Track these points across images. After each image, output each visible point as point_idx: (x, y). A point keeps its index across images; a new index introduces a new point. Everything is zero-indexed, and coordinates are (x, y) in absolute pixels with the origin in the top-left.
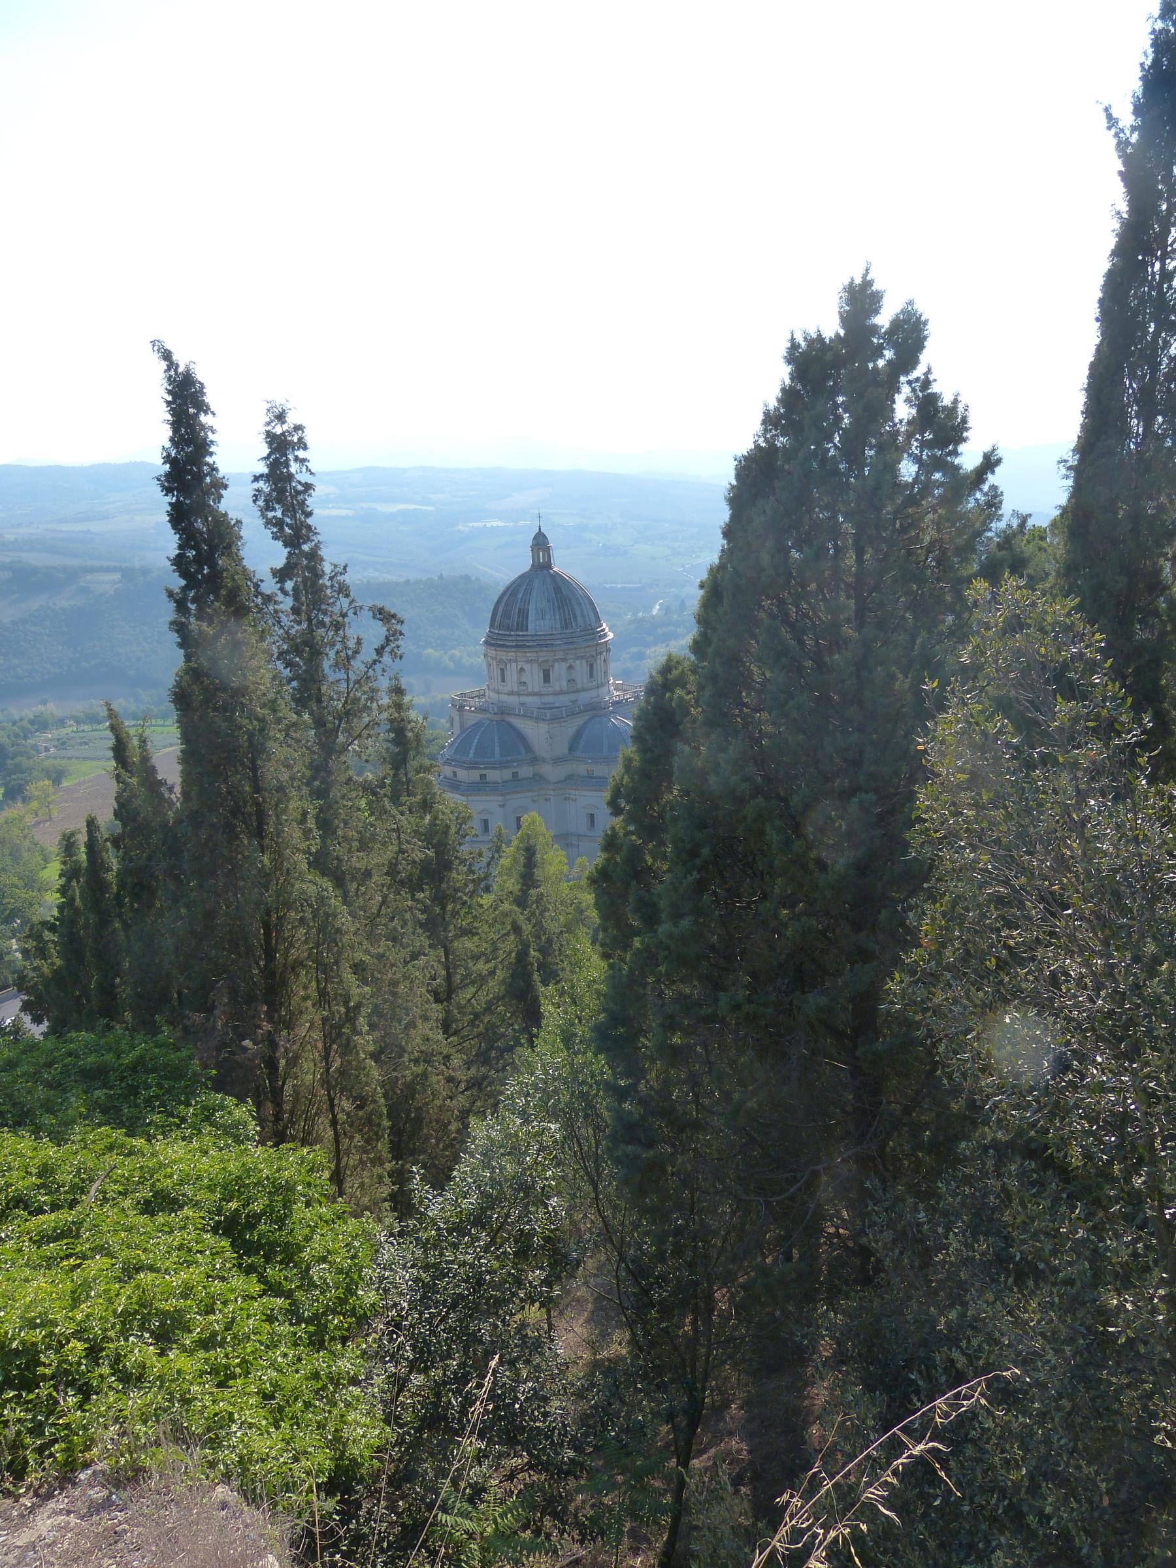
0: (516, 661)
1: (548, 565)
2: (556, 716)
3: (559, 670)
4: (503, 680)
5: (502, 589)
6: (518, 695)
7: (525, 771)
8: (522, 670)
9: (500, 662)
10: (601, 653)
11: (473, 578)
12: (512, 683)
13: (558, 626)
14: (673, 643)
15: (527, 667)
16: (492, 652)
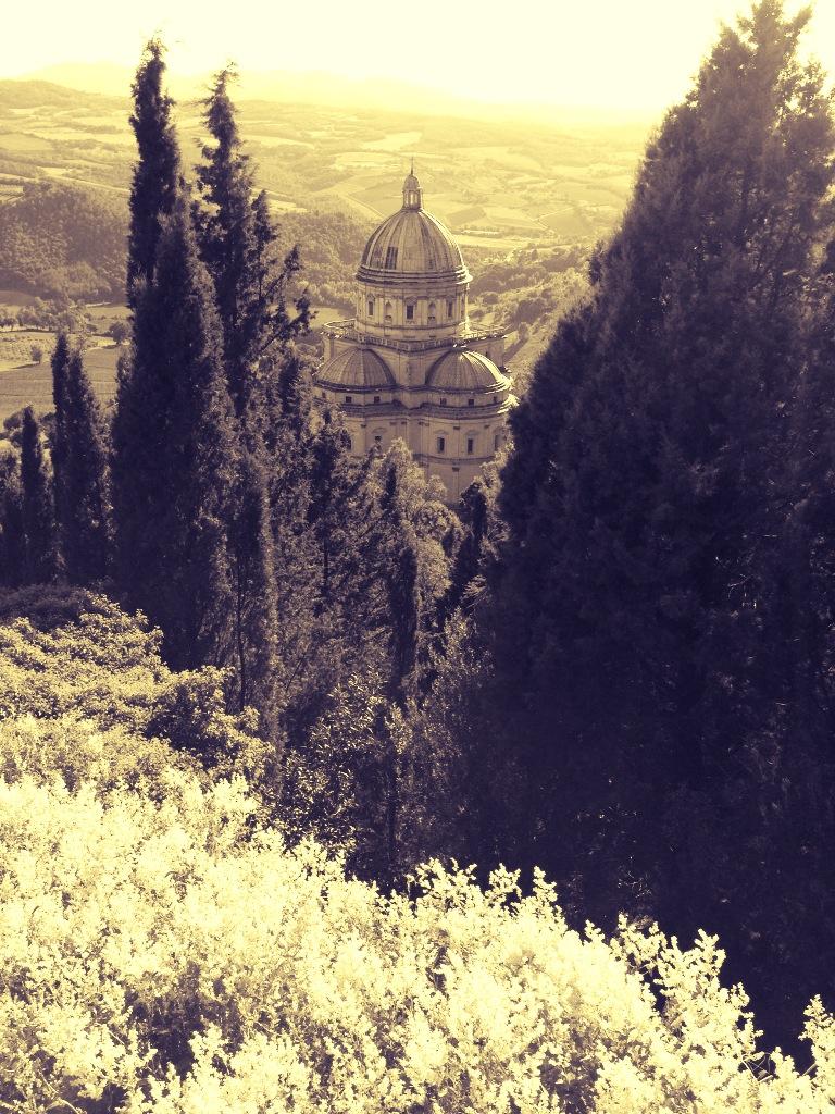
0: (383, 297)
1: (416, 208)
2: (416, 349)
3: (422, 308)
4: (371, 313)
5: (372, 230)
6: (383, 327)
7: (386, 397)
8: (388, 305)
9: (370, 296)
10: (460, 294)
11: (346, 216)
12: (378, 317)
13: (423, 266)
14: (523, 290)
15: (393, 302)
16: (361, 286)
